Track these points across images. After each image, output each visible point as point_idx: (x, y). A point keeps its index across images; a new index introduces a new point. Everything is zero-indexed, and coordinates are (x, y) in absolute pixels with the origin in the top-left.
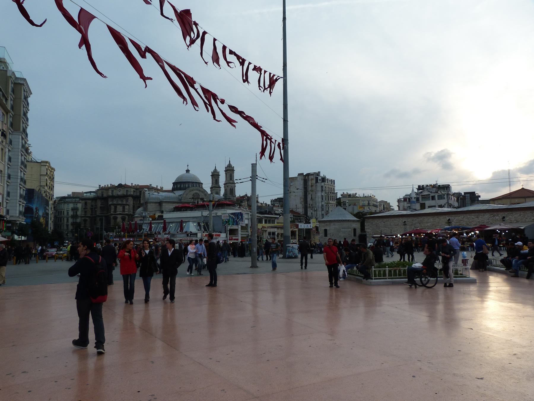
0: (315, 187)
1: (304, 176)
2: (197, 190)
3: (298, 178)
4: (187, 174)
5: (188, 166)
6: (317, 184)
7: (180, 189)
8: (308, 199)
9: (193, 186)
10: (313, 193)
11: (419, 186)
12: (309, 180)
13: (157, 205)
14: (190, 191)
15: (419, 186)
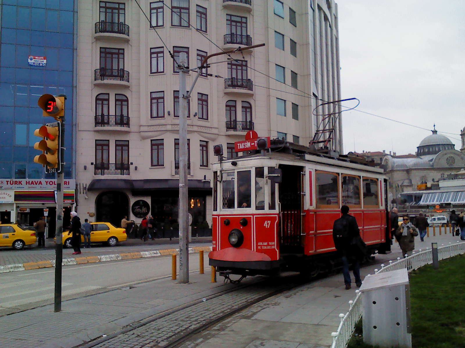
2: (451, 153)
4: (435, 135)
5: (434, 126)
7: (429, 153)
9: (445, 149)
13: (405, 172)
14: (443, 155)
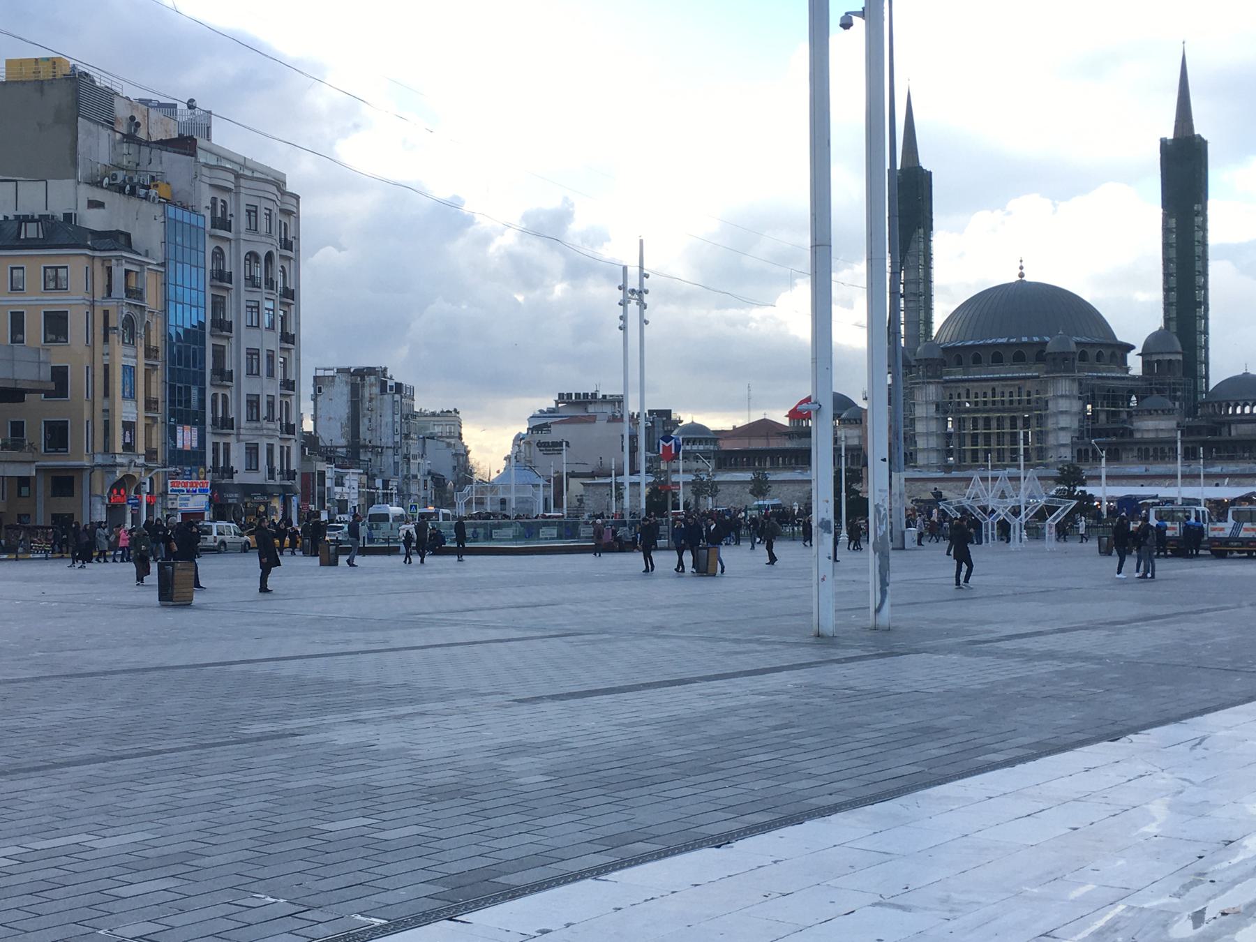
0: (379, 402)
1: (352, 374)
3: (337, 379)
6: (386, 396)
8: (361, 427)
10: (374, 416)
11: (561, 396)
12: (363, 386)
15: (561, 396)
